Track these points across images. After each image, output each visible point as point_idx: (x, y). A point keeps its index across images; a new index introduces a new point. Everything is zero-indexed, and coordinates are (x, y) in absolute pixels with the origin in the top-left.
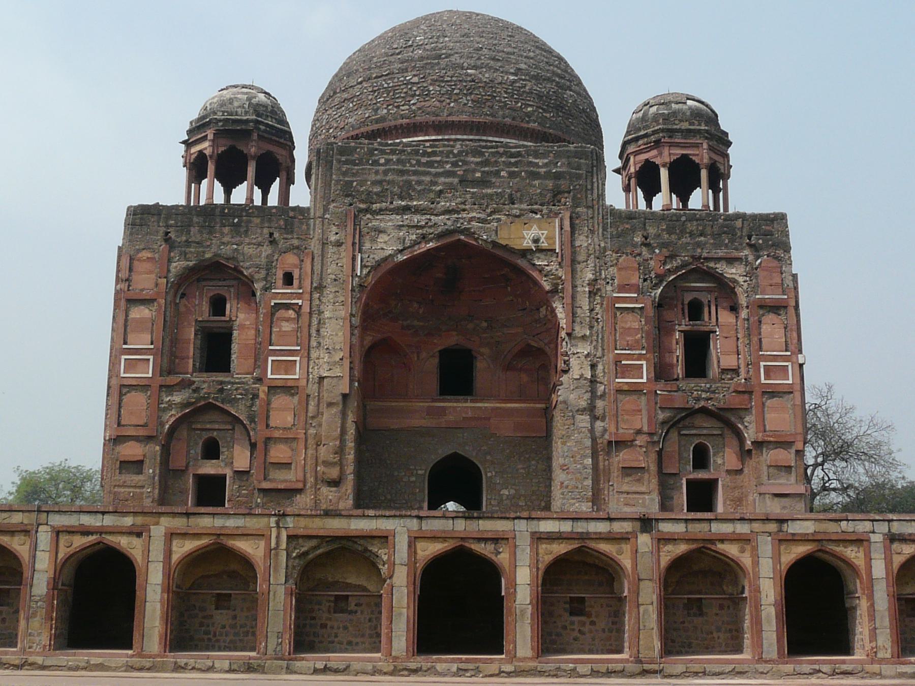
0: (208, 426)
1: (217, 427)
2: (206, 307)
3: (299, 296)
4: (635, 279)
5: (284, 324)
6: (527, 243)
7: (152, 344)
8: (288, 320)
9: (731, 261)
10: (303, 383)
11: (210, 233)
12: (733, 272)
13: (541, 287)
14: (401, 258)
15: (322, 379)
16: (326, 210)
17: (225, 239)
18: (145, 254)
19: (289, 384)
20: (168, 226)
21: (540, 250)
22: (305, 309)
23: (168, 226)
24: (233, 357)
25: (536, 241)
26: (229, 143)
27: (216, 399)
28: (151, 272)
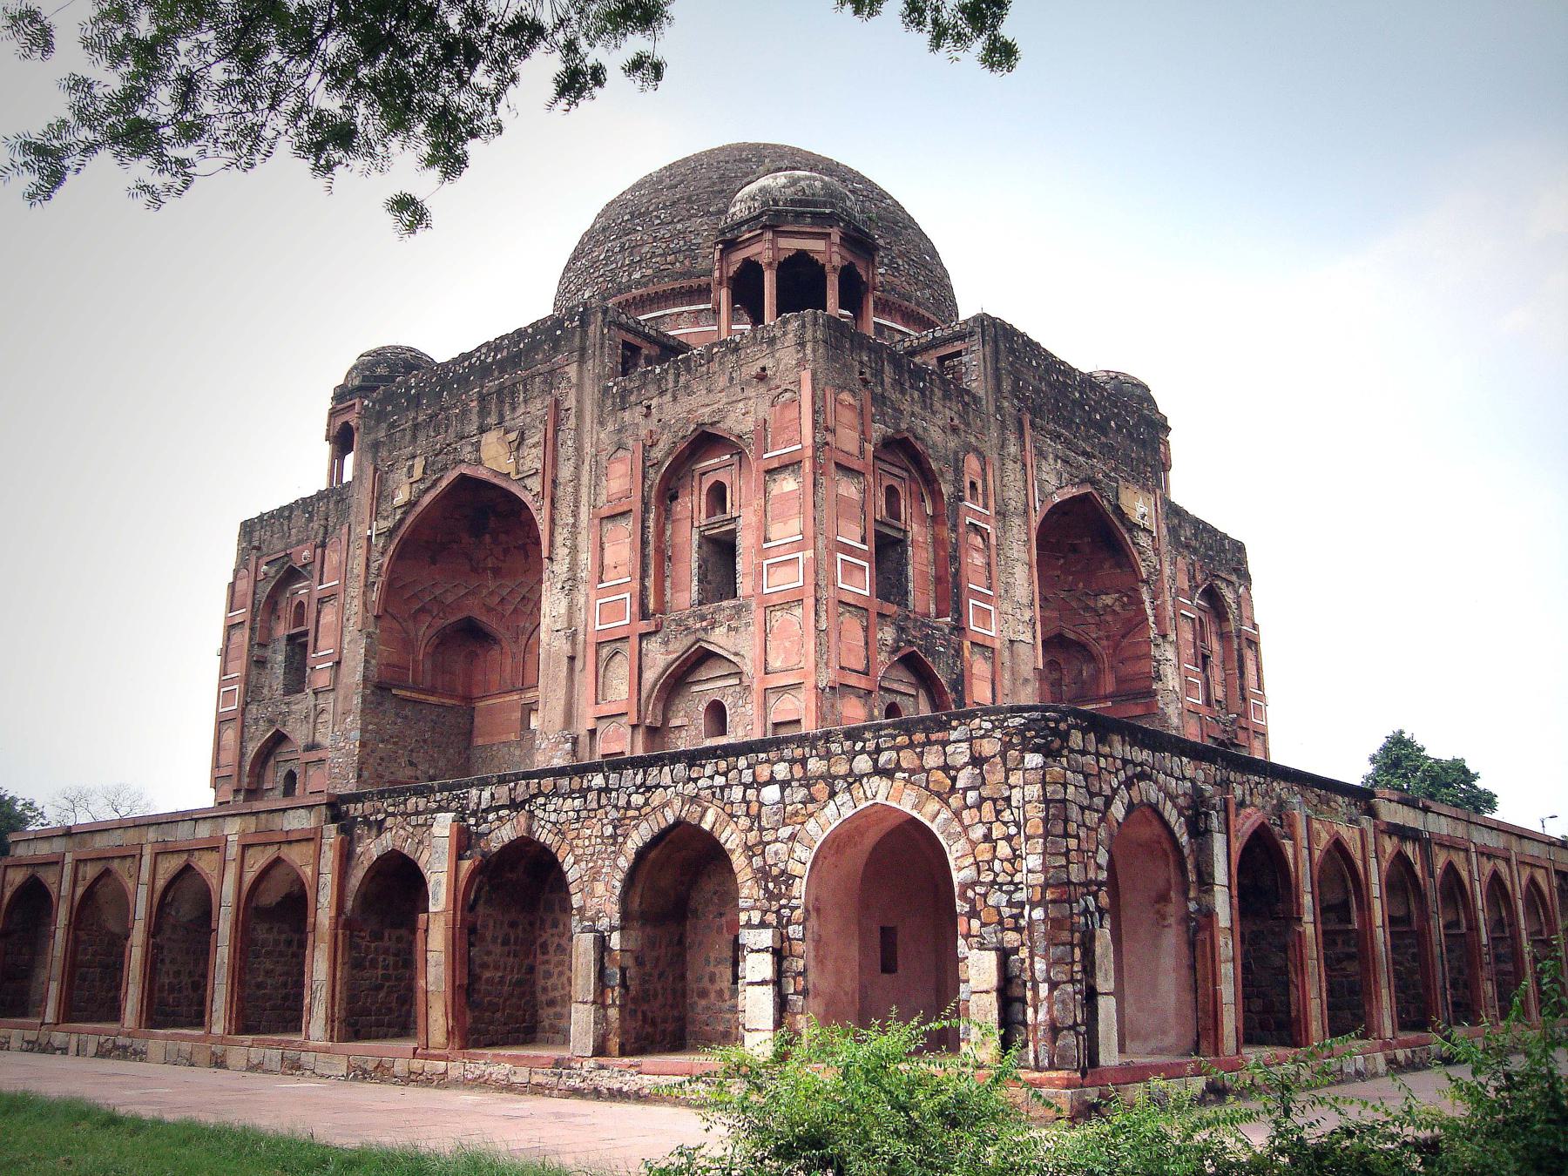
0: (895, 686)
1: (902, 688)
2: (882, 502)
3: (986, 519)
4: (1186, 587)
5: (975, 555)
6: (1136, 519)
7: (863, 541)
8: (977, 550)
9: (1229, 583)
10: (997, 645)
11: (903, 392)
12: (1229, 596)
13: (1135, 571)
14: (1057, 500)
15: (1011, 642)
16: (999, 409)
17: (917, 409)
18: (846, 397)
19: (988, 643)
20: (861, 362)
21: (1145, 529)
22: (993, 541)
23: (861, 362)
24: (911, 585)
25: (1143, 516)
26: (850, 258)
27: (920, 647)
28: (852, 428)
